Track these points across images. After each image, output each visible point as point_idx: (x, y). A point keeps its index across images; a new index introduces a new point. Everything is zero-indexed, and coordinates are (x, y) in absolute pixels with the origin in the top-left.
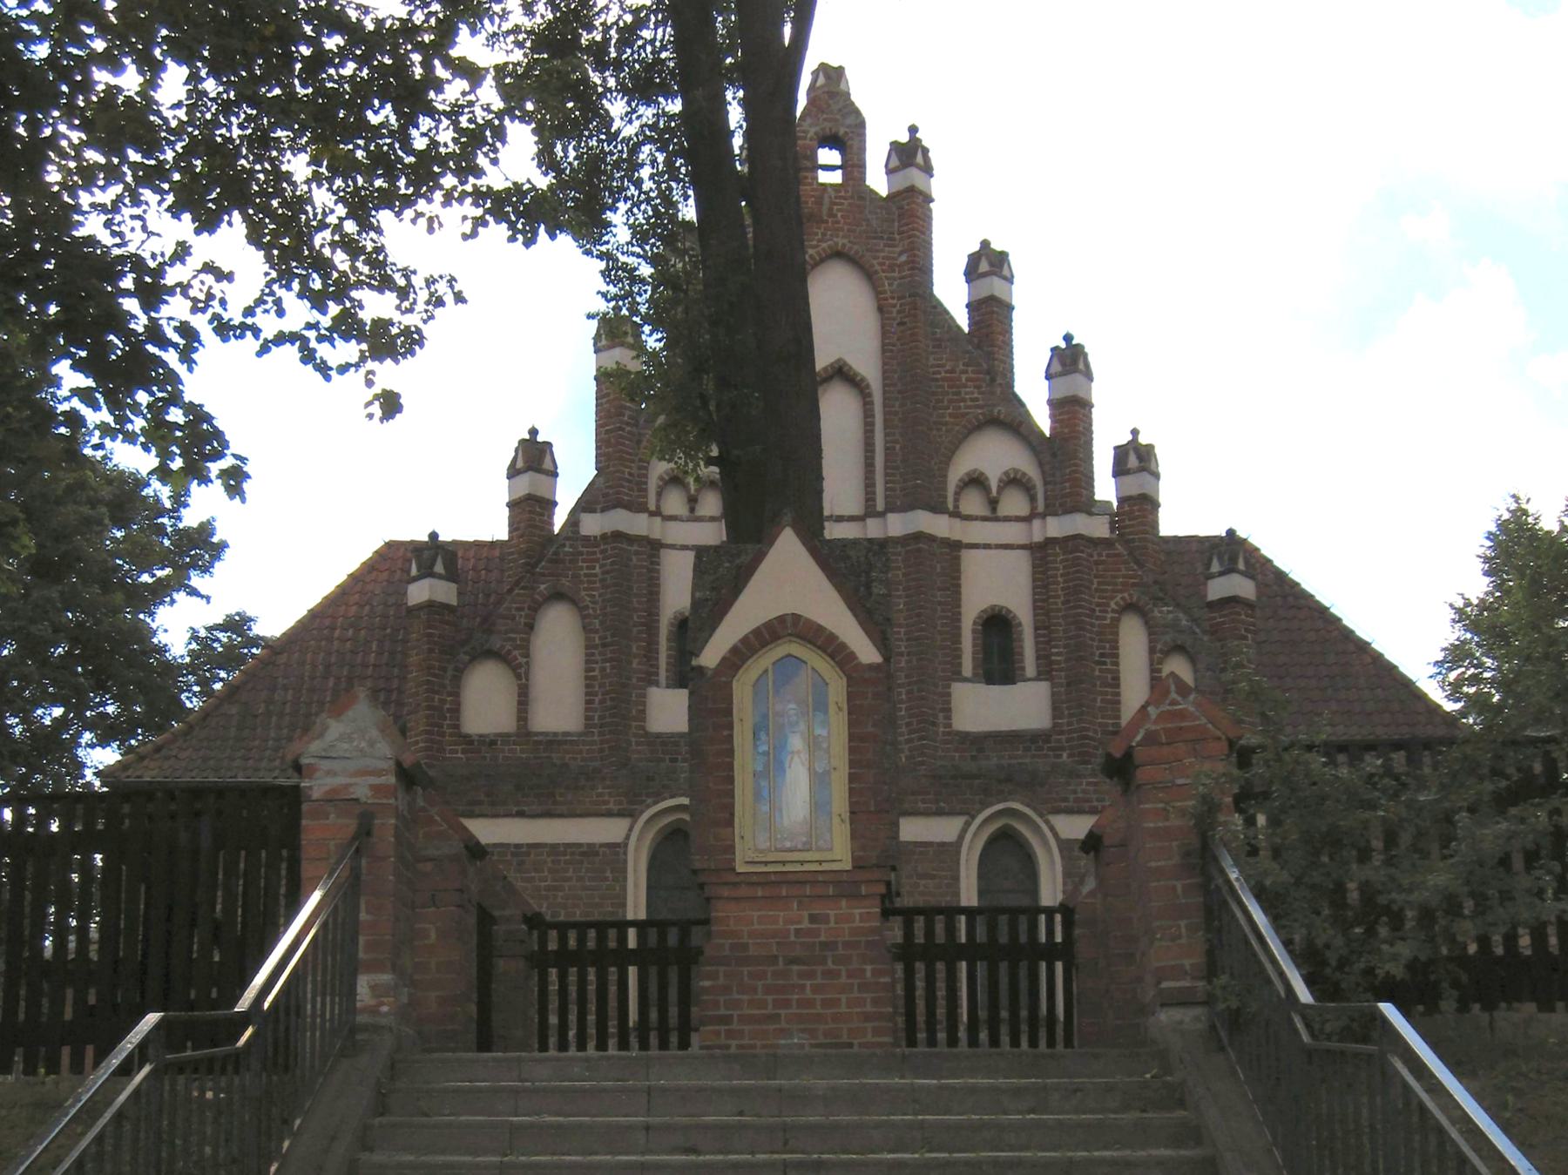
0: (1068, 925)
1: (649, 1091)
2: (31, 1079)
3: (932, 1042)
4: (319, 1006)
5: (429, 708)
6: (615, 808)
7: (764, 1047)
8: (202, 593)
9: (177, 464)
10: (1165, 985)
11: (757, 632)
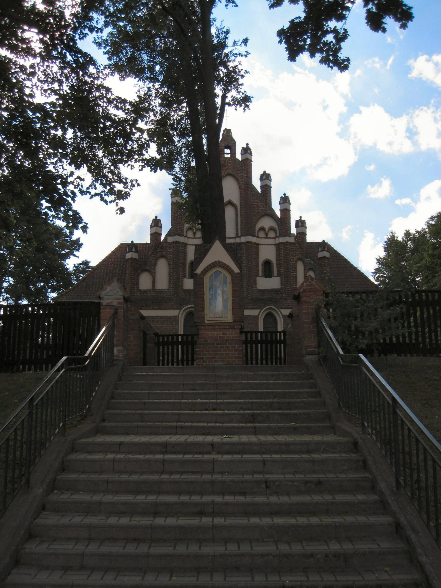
0: (285, 335)
1: (184, 375)
2: (36, 372)
3: (252, 363)
4: (105, 355)
5: (131, 283)
6: (176, 307)
7: (211, 365)
8: (77, 256)
9: (71, 225)
10: (308, 350)
11: (210, 265)
